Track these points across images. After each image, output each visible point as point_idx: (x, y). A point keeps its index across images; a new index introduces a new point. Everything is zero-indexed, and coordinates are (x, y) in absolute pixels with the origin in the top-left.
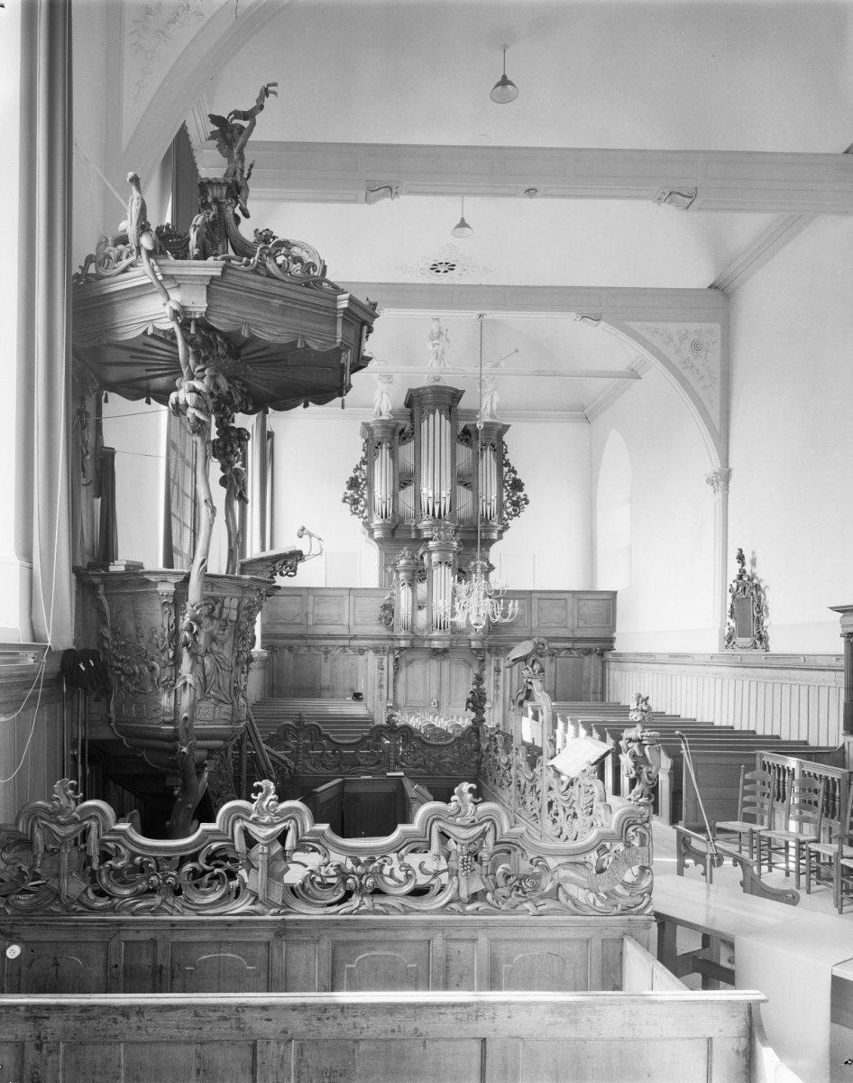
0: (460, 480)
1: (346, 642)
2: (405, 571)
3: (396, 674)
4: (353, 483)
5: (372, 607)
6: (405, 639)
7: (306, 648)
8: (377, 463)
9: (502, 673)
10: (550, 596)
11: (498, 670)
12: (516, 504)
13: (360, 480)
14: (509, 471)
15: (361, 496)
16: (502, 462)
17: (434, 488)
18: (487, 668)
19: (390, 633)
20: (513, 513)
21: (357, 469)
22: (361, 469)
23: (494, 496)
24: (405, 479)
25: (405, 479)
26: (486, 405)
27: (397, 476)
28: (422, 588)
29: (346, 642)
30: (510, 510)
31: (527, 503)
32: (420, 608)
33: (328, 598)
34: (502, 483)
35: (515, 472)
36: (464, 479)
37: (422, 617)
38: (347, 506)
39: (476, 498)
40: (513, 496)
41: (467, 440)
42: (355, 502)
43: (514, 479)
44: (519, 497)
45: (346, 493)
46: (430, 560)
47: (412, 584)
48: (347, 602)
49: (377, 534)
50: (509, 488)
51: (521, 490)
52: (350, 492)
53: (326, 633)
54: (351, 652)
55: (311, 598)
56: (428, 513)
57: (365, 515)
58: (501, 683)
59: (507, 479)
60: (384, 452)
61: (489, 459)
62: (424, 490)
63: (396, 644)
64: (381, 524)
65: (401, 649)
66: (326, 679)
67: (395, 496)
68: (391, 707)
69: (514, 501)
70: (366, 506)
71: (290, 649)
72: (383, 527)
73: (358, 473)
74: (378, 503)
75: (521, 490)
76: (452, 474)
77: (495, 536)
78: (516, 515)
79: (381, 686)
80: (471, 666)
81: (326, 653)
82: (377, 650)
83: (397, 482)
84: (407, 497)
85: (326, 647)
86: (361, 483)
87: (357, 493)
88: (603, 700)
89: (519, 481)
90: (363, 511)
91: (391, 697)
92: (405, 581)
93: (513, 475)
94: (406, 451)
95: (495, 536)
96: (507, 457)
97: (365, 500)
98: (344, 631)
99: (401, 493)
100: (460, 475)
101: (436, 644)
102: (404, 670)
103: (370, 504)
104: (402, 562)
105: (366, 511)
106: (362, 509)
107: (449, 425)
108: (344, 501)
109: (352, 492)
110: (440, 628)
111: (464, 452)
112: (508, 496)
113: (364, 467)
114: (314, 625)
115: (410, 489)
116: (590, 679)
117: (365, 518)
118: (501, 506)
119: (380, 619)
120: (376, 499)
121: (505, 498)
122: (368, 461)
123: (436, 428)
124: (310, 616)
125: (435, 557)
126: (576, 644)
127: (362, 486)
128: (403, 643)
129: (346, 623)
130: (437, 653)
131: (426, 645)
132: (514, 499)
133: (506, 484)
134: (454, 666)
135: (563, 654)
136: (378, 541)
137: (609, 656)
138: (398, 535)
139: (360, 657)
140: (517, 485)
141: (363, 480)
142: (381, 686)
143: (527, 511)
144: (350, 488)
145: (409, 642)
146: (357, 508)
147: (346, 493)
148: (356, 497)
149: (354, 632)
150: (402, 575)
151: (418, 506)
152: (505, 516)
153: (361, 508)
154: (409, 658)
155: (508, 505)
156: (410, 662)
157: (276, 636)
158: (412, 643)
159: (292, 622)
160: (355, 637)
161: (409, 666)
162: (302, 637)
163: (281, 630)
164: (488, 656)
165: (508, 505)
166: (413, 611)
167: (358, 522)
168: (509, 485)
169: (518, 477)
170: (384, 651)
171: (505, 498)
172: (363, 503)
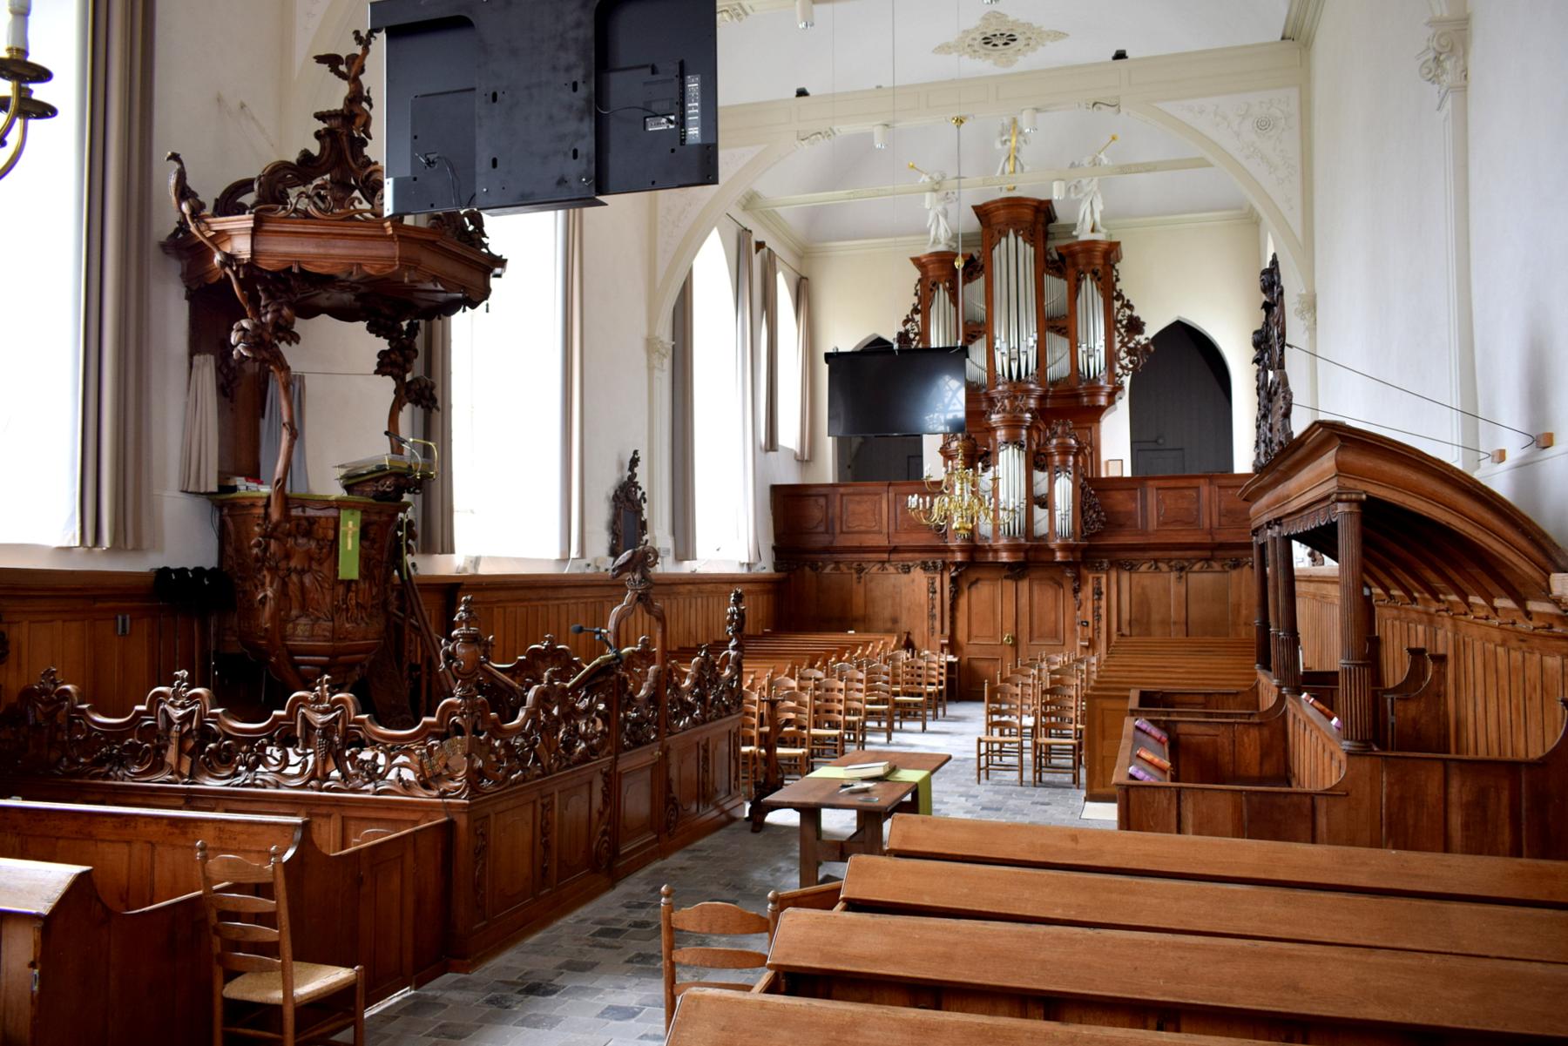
9: (1104, 597)
11: (1098, 593)
14: (1123, 306)
16: (1110, 293)
21: (906, 322)
23: (1100, 344)
26: (1086, 217)
29: (885, 556)
30: (1125, 362)
35: (1130, 307)
36: (1057, 324)
51: (1141, 332)
54: (891, 569)
58: (1103, 611)
60: (941, 297)
61: (1089, 291)
62: (998, 344)
65: (958, 565)
66: (858, 608)
75: (1141, 332)
77: (1103, 401)
79: (933, 617)
80: (1061, 585)
81: (860, 570)
89: (1138, 319)
91: (947, 631)
93: (1128, 312)
94: (973, 292)
95: (1103, 401)
96: (1119, 286)
100: (1051, 319)
101: (1004, 557)
107: (1030, 251)
111: (1056, 287)
116: (1239, 605)
121: (1118, 346)
123: (1014, 257)
126: (1217, 553)
128: (959, 557)
131: (990, 557)
132: (1131, 345)
142: (933, 617)
149: (896, 542)
152: (1119, 371)
154: (973, 576)
155: (1122, 354)
156: (972, 584)
161: (973, 589)
164: (1084, 572)
165: (1122, 354)
170: (936, 568)
171: (1118, 346)
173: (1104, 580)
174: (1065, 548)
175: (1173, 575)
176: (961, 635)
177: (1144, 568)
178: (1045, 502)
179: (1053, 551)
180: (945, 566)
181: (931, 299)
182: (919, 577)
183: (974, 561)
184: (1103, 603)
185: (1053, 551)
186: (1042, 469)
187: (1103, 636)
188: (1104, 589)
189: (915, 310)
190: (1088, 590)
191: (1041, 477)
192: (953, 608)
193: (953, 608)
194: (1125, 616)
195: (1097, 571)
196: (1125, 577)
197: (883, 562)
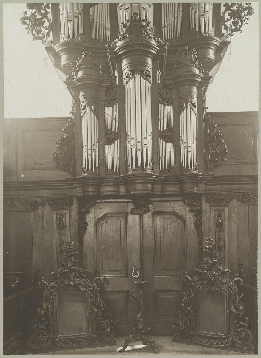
15: (45, 16)
20: (234, 27)
42: (37, 23)
45: (25, 13)
78: (239, 30)
90: (48, 35)
97: (48, 21)
105: (51, 34)
108: (24, 23)
109: (33, 11)
146: (39, 32)
147: (25, 13)
148: (39, 17)
155: (227, 17)
165: (227, 17)
167: (40, 47)
172: (47, 24)
178: (171, 136)
186: (167, 102)
191: (166, 111)
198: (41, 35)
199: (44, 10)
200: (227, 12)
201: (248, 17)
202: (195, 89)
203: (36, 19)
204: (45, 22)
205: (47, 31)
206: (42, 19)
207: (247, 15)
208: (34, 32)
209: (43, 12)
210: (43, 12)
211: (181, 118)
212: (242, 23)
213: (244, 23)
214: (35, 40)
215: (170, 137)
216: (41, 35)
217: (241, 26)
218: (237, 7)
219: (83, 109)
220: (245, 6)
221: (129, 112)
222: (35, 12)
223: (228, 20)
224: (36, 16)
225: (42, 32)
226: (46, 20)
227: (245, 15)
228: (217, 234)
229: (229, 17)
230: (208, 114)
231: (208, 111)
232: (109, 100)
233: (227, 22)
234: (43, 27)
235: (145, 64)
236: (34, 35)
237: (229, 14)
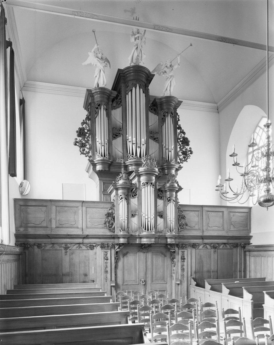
0: (152, 135)
1: (80, 241)
2: (123, 188)
3: (116, 263)
4: (81, 133)
5: (99, 215)
6: (123, 238)
7: (51, 245)
8: (98, 120)
9: (186, 260)
10: (213, 209)
11: (183, 259)
12: (185, 153)
13: (86, 131)
14: (181, 132)
15: (87, 141)
16: (177, 127)
17: (136, 139)
18: (177, 256)
19: (112, 234)
20: (183, 159)
21: (83, 123)
22: (86, 123)
24: (116, 132)
25: (116, 132)
27: (111, 130)
28: (134, 201)
29: (80, 241)
30: (181, 157)
31: (191, 153)
32: (133, 216)
33: (66, 208)
34: (176, 139)
35: (184, 133)
36: (154, 135)
37: (135, 221)
38: (77, 148)
39: (161, 147)
40: (183, 148)
41: (155, 110)
42: (83, 146)
43: (184, 138)
44: (186, 149)
45: (76, 139)
46: (139, 182)
47: (127, 199)
48: (80, 211)
49: (99, 168)
50: (180, 143)
51: (188, 145)
52: (79, 139)
53: (66, 234)
54: (84, 248)
55: (54, 208)
56: (133, 154)
57: (90, 154)
58: (185, 267)
59: (179, 137)
63: (116, 241)
64: (101, 160)
65: (120, 245)
66: (66, 268)
67: (110, 143)
68: (113, 286)
69: (183, 151)
70: (90, 149)
71: (39, 246)
72: (103, 162)
73: (84, 126)
74: (98, 145)
75: (188, 145)
76: (146, 131)
78: (185, 160)
80: (165, 256)
81: (66, 248)
82: (103, 246)
83: (111, 134)
84: (118, 143)
85: (66, 244)
86: (87, 133)
87: (85, 141)
88: (245, 276)
89: (187, 139)
90: (89, 152)
91: (113, 279)
92: (123, 196)
93: (183, 135)
94: (117, 114)
96: (179, 123)
97: (89, 144)
98: (78, 232)
99: (114, 142)
100: (151, 132)
101: (145, 241)
102: (122, 259)
103: (93, 148)
104: (121, 182)
105: (90, 152)
106: (88, 150)
108: (75, 145)
109: (81, 138)
110: (148, 230)
112: (180, 148)
113: (89, 122)
114: (57, 227)
115: (119, 140)
116: (237, 263)
117: (90, 157)
118: (176, 155)
119: (105, 223)
120: (97, 143)
121: (178, 149)
122: (91, 118)
124: (54, 222)
125: (143, 179)
127: (87, 135)
128: (122, 241)
129: (80, 226)
130: (143, 248)
131: (138, 241)
132: (184, 150)
133: (179, 140)
134: (154, 256)
135: (221, 247)
136: (100, 174)
137: (248, 248)
138: (109, 171)
139: (91, 251)
140: (186, 142)
141: (88, 131)
143: (192, 158)
144: (79, 136)
145: (126, 240)
146: (84, 150)
147: (76, 139)
148: (84, 142)
149: (86, 233)
150: (120, 192)
151: (125, 150)
153: (87, 150)
154: (125, 251)
156: (125, 255)
157: (27, 236)
158: (128, 241)
159: (40, 225)
160: (87, 237)
162: (48, 237)
163: (31, 231)
164: (177, 249)
165: (180, 154)
166: (128, 218)
168: (181, 141)
169: (186, 136)
171: (178, 149)
172: (88, 146)
173: (186, 253)
174: (175, 237)
175: (213, 250)
176: (120, 281)
177: (201, 247)
179: (166, 238)
180: (113, 246)
181: (97, 113)
182: (99, 252)
183: (131, 245)
184: (185, 263)
185: (166, 238)
186: (161, 198)
187: (185, 279)
188: (186, 257)
189: (88, 118)
190: (178, 258)
191: (160, 202)
192: (116, 267)
193: (116, 267)
194: (194, 269)
195: (183, 248)
196: (194, 250)
197: (79, 244)
198: (85, 152)
199: (87, 138)
200: (181, 151)
201: (190, 155)
202: (174, 193)
203: (83, 143)
204: (87, 145)
205: (88, 150)
206: (85, 143)
207: (190, 154)
208: (81, 150)
209: (86, 139)
210: (86, 139)
211: (168, 207)
212: (187, 158)
213: (188, 158)
214: (82, 155)
215: (162, 216)
216: (85, 152)
217: (187, 159)
218: (185, 150)
219: (121, 199)
220: (189, 149)
221: (152, 206)
222: (82, 139)
223: (181, 155)
224: (82, 141)
225: (86, 150)
226: (88, 144)
227: (189, 154)
228: (182, 263)
229: (181, 154)
230: (179, 205)
231: (179, 204)
232: (133, 195)
233: (180, 156)
234: (86, 148)
235: (151, 180)
236: (81, 151)
237: (181, 153)
